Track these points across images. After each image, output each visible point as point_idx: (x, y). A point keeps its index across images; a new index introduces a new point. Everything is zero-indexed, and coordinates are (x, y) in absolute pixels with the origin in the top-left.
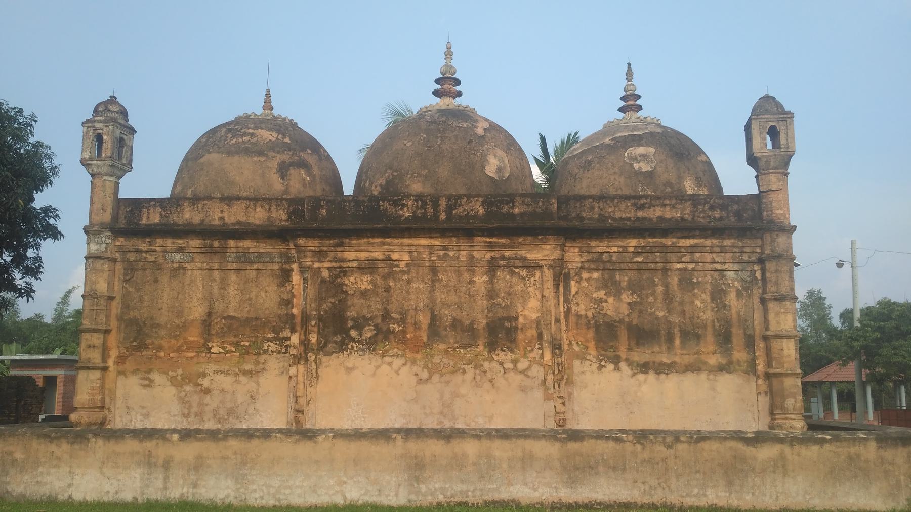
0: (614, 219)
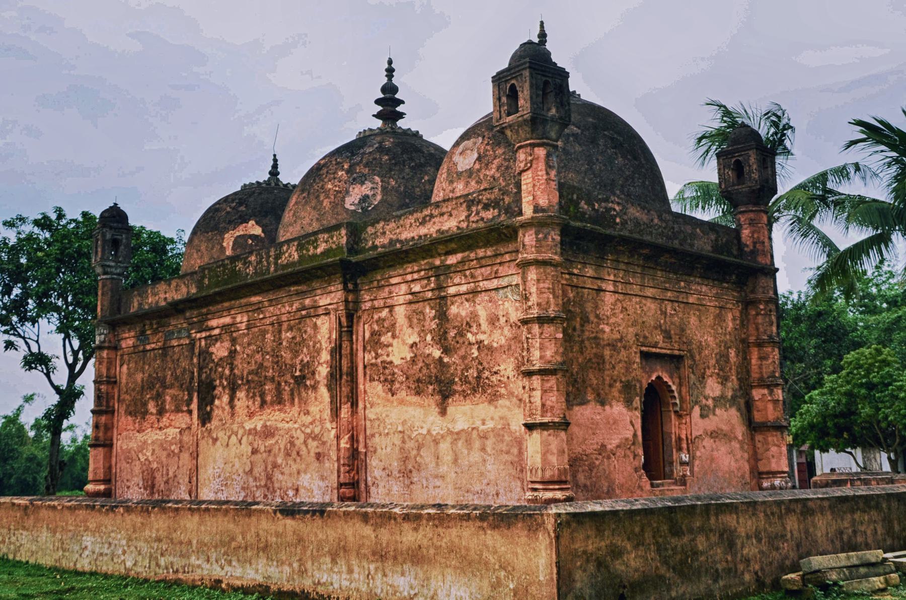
0: (401, 242)
